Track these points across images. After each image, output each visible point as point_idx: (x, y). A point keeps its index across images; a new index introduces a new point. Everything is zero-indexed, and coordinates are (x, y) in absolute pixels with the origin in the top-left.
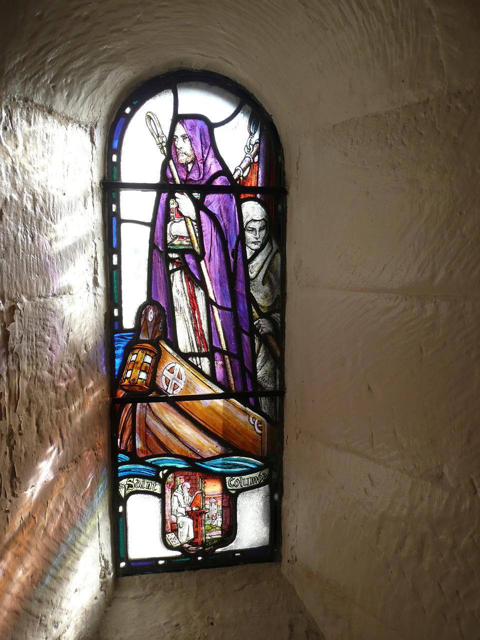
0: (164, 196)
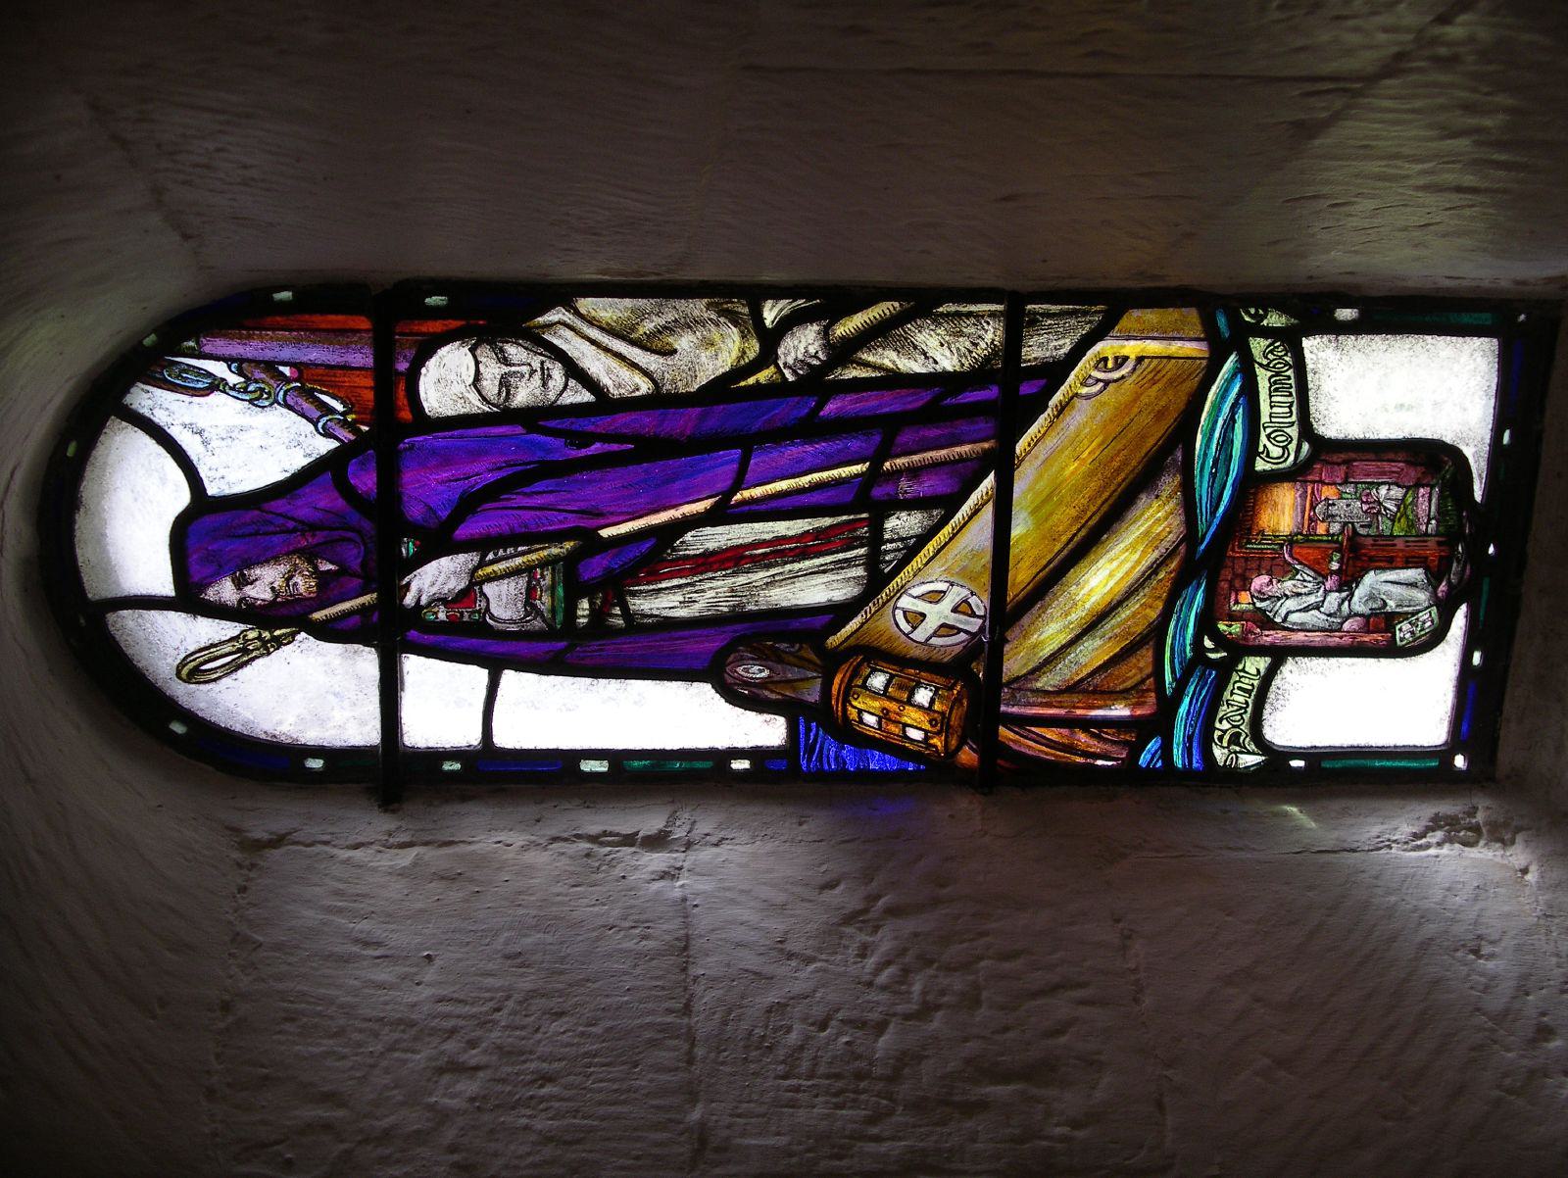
0: (413, 634)
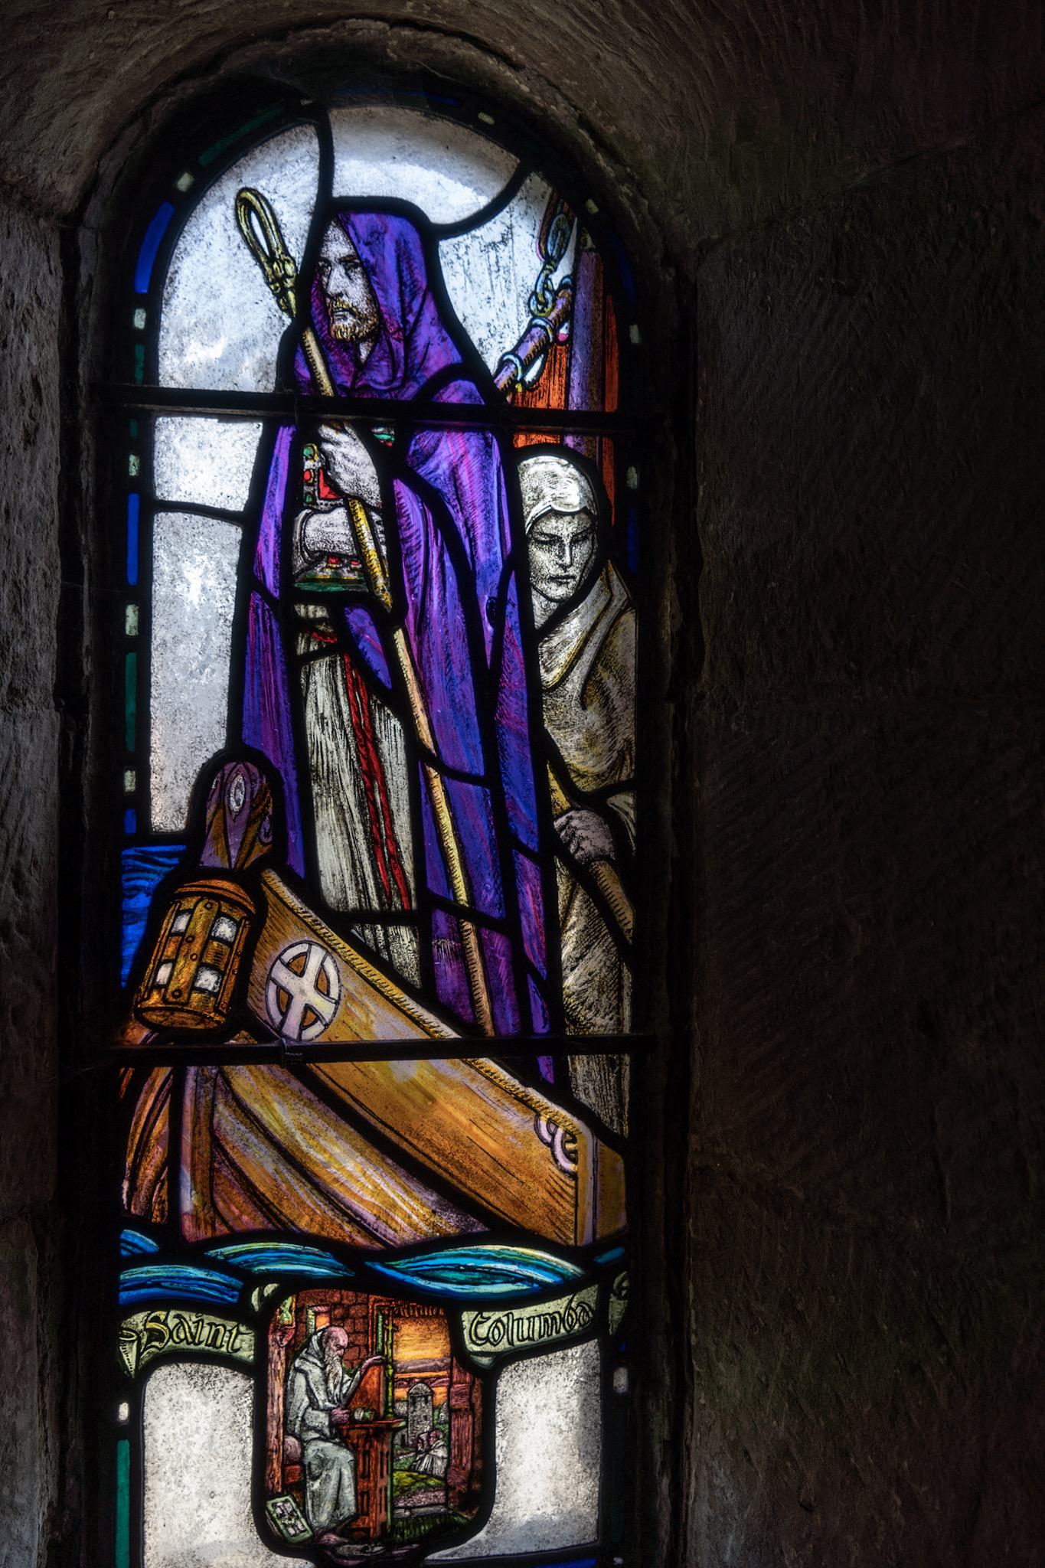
0: (285, 436)
